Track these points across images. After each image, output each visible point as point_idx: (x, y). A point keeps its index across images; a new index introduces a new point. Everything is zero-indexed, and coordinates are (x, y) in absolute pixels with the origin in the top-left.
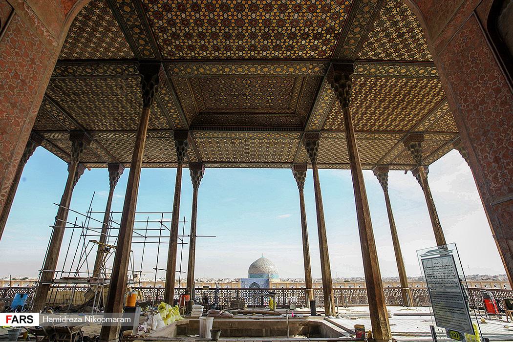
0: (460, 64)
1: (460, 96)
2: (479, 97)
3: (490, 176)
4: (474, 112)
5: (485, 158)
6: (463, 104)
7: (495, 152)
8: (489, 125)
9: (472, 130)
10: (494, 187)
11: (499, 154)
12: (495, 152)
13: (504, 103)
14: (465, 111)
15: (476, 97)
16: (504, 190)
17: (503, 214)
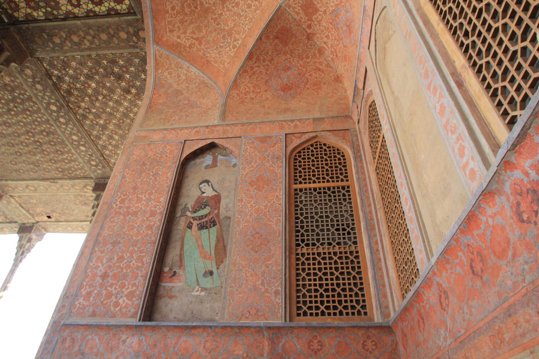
0: (144, 168)
1: (121, 194)
2: (136, 207)
3: (85, 289)
4: (122, 217)
5: (95, 268)
6: (118, 203)
7: (110, 267)
8: (124, 238)
9: (106, 232)
10: (80, 303)
11: (111, 271)
12: (110, 267)
13: (149, 227)
14: (115, 210)
15: (133, 205)
16: (88, 311)
17: (66, 339)
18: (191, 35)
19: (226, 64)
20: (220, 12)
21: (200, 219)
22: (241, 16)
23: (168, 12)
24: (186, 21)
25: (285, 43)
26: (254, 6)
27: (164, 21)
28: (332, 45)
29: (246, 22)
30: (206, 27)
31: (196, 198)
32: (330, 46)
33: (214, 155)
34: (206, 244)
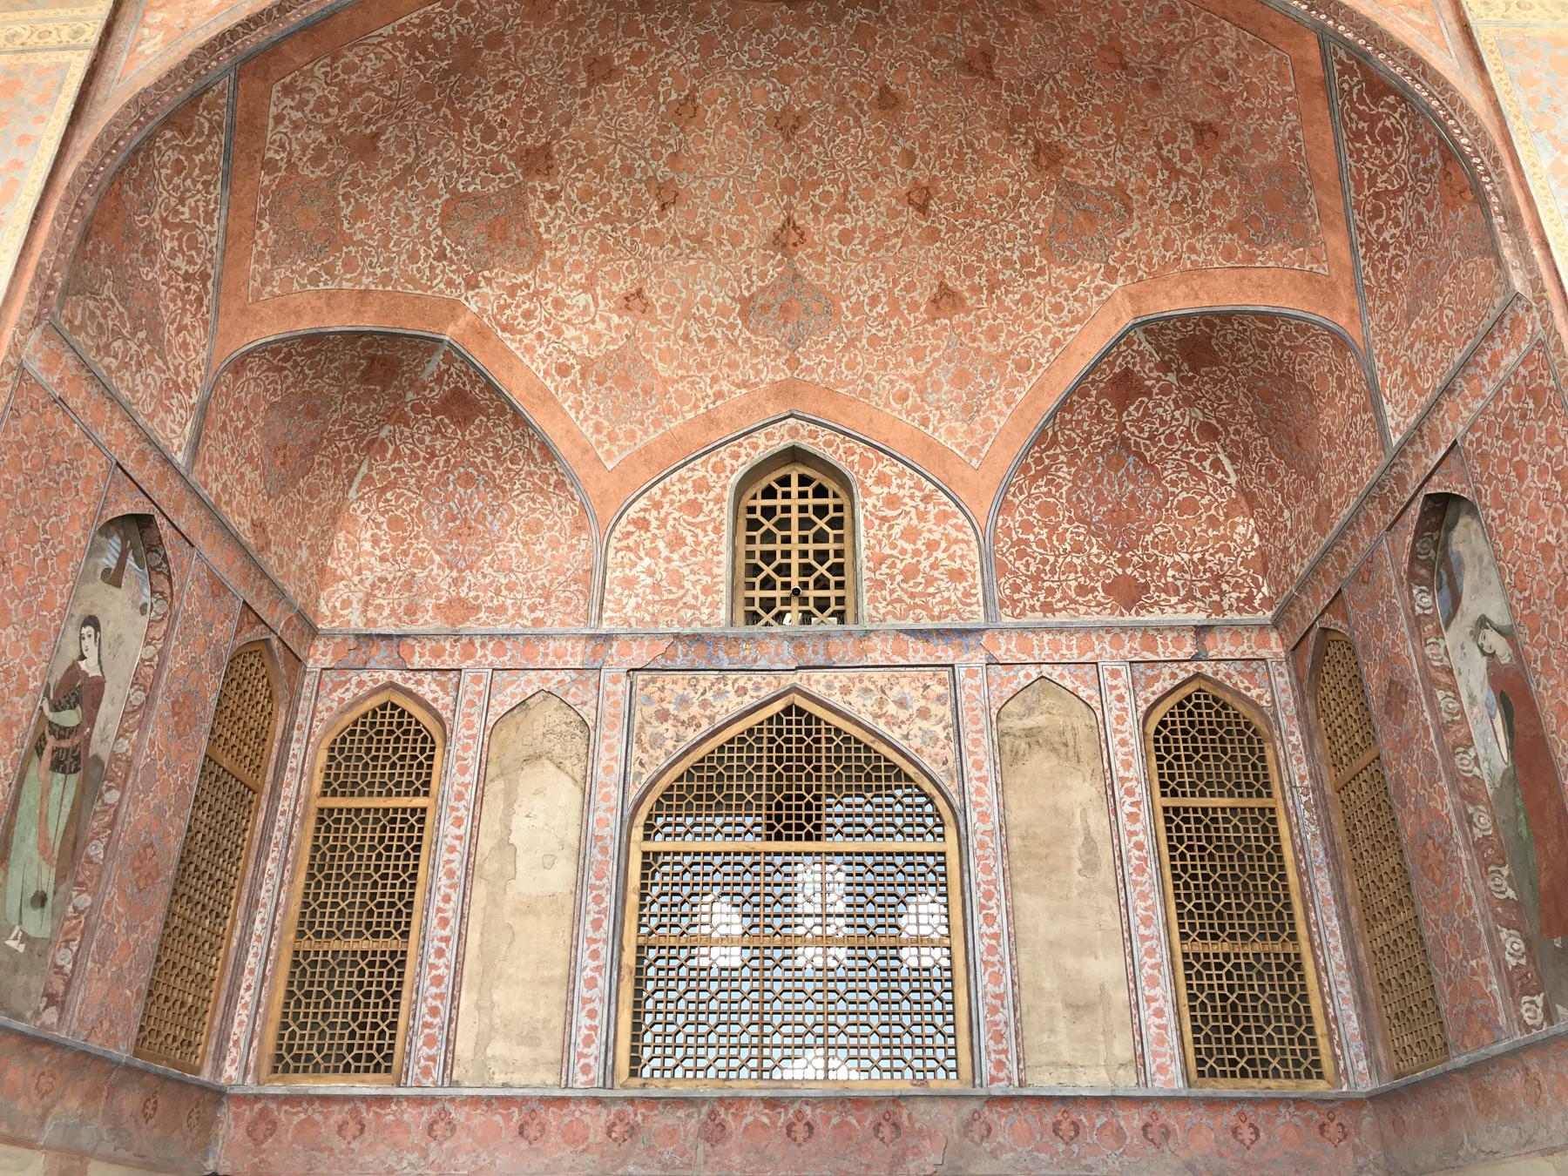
18: (295, 146)
19: (269, 289)
20: (375, 184)
21: (60, 737)
22: (386, 247)
23: (335, 59)
24: (327, 115)
25: (366, 378)
26: (418, 269)
27: (307, 59)
28: (400, 470)
29: (378, 271)
30: (328, 170)
31: (69, 663)
32: (396, 465)
33: (124, 539)
34: (53, 814)
